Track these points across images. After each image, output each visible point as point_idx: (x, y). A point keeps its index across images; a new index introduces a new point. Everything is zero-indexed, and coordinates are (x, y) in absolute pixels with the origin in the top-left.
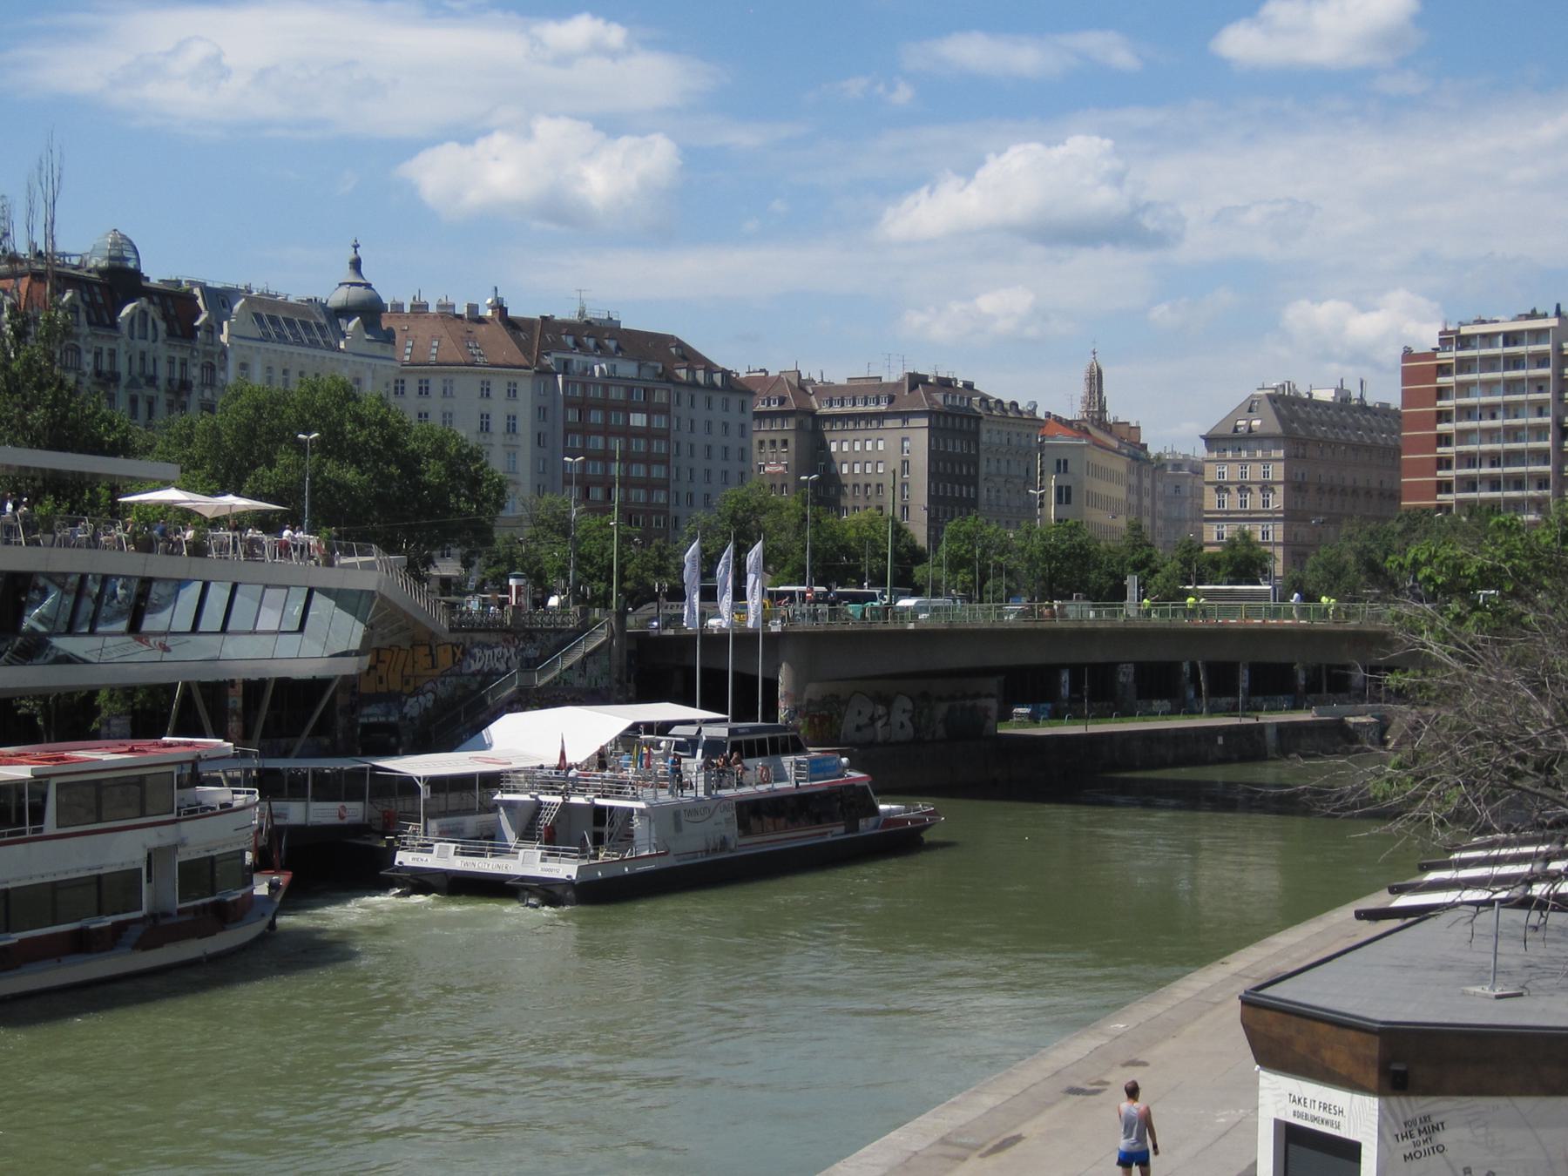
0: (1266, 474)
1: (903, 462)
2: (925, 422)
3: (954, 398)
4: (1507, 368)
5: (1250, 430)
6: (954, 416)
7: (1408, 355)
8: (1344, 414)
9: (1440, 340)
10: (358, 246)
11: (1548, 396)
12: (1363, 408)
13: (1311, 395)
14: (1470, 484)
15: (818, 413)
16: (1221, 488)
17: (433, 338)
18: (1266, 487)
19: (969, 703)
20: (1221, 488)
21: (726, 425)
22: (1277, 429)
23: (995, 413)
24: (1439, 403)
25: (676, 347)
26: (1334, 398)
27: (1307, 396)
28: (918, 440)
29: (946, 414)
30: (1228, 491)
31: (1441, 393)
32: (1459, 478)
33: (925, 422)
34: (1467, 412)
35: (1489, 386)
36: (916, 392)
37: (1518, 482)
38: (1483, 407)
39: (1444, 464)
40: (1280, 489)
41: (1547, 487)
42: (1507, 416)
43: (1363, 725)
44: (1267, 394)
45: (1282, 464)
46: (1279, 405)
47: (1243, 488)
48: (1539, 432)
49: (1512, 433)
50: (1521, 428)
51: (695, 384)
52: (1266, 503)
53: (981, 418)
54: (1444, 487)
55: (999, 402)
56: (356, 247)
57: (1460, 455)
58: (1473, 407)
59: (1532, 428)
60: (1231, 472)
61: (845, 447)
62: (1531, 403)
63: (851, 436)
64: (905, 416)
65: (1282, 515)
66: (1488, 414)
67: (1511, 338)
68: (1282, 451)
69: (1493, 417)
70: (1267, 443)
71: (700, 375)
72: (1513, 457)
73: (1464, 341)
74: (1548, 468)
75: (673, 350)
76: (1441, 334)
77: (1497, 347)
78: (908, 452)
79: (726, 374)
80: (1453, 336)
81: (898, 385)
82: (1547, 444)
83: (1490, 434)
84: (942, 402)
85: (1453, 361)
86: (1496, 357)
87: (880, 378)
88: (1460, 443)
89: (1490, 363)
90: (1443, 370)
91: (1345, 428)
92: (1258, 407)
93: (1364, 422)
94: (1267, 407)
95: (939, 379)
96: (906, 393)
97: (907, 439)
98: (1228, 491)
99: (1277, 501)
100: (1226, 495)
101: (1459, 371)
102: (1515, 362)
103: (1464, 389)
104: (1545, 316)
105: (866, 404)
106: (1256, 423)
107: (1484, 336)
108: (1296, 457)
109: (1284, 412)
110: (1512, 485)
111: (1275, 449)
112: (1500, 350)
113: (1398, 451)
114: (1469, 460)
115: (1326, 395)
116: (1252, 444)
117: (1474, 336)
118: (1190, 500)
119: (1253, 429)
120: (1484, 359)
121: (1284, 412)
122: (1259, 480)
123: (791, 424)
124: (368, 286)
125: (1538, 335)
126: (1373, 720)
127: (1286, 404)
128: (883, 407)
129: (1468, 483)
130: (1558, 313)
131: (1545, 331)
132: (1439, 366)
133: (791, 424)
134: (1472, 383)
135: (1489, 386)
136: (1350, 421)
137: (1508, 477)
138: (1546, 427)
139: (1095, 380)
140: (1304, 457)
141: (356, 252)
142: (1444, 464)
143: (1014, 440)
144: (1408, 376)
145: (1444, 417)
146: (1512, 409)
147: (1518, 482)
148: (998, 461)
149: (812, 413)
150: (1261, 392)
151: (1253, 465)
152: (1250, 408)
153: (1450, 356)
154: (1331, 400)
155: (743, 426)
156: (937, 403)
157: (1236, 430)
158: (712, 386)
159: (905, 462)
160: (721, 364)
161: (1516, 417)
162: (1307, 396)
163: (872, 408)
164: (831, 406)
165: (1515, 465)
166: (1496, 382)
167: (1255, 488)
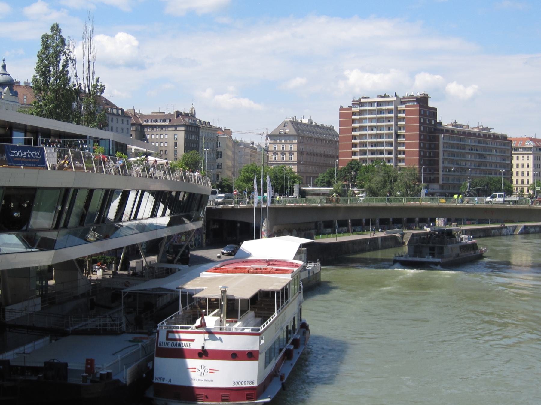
0: (291, 148)
1: (175, 142)
2: (183, 128)
3: (192, 120)
4: (378, 114)
5: (285, 133)
6: (192, 126)
7: (342, 108)
8: (312, 128)
9: (352, 103)
10: (5, 60)
11: (393, 123)
12: (316, 126)
13: (302, 121)
14: (364, 153)
15: (143, 124)
16: (275, 153)
17: (24, 95)
18: (291, 153)
19: (309, 232)
20: (275, 153)
21: (122, 129)
22: (294, 133)
23: (204, 126)
24: (353, 125)
25: (105, 100)
26: (308, 122)
27: (300, 122)
28: (181, 135)
29: (190, 126)
30: (277, 154)
31: (353, 122)
32: (360, 151)
33: (183, 128)
34: (362, 128)
35: (371, 120)
36: (179, 117)
37: (381, 153)
38: (369, 127)
40: (296, 154)
41: (391, 154)
42: (377, 130)
43: (398, 237)
44: (290, 121)
45: (297, 145)
47: (283, 153)
48: (389, 136)
49: (380, 136)
50: (383, 134)
51: (113, 114)
53: (200, 127)
54: (354, 153)
55: (204, 122)
56: (4, 60)
57: (361, 143)
59: (387, 134)
60: (279, 147)
61: (153, 137)
62: (386, 125)
63: (155, 133)
64: (175, 126)
65: (296, 162)
66: (370, 129)
67: (379, 104)
68: (297, 141)
69: (372, 130)
70: (286, 138)
71: (115, 111)
73: (362, 104)
74: (392, 148)
75: (104, 101)
76: (352, 101)
77: (374, 106)
78: (177, 139)
79: (122, 110)
81: (170, 115)
82: (392, 140)
83: (371, 136)
84: (188, 122)
85: (359, 111)
86: (374, 110)
87: (164, 113)
88: (361, 139)
89: (371, 112)
90: (354, 114)
91: (317, 133)
92: (287, 125)
94: (290, 125)
95: (185, 113)
96: (175, 118)
97: (177, 135)
98: (277, 154)
99: (295, 157)
100: (277, 155)
101: (361, 114)
102: (380, 112)
103: (362, 120)
104: (392, 97)
105: (161, 122)
106: (287, 131)
107: (369, 102)
108: (301, 142)
109: (296, 127)
110: (379, 153)
112: (375, 107)
113: (338, 142)
114: (364, 144)
115: (305, 121)
117: (366, 103)
118: (244, 156)
119: (286, 133)
120: (370, 110)
121: (296, 127)
122: (288, 150)
123: (134, 128)
124: (9, 75)
125: (389, 103)
126: (400, 235)
127: (295, 123)
128: (167, 123)
129: (363, 152)
130: (396, 95)
131: (392, 101)
132: (353, 112)
133: (134, 128)
134: (366, 119)
135: (371, 120)
137: (378, 150)
138: (392, 134)
139: (455, 121)
140: (303, 143)
141: (4, 62)
143: (210, 136)
144: (342, 116)
146: (379, 128)
147: (381, 153)
148: (208, 143)
149: (140, 125)
150: (287, 120)
151: (286, 145)
152: (285, 125)
153: (358, 109)
154: (307, 123)
155: (128, 129)
156: (187, 122)
157: (280, 133)
158: (118, 115)
159: (176, 143)
160: (119, 107)
161: (380, 130)
162: (300, 122)
163: (163, 123)
164: (156, 122)
165: (380, 147)
166: (374, 118)
167: (287, 153)
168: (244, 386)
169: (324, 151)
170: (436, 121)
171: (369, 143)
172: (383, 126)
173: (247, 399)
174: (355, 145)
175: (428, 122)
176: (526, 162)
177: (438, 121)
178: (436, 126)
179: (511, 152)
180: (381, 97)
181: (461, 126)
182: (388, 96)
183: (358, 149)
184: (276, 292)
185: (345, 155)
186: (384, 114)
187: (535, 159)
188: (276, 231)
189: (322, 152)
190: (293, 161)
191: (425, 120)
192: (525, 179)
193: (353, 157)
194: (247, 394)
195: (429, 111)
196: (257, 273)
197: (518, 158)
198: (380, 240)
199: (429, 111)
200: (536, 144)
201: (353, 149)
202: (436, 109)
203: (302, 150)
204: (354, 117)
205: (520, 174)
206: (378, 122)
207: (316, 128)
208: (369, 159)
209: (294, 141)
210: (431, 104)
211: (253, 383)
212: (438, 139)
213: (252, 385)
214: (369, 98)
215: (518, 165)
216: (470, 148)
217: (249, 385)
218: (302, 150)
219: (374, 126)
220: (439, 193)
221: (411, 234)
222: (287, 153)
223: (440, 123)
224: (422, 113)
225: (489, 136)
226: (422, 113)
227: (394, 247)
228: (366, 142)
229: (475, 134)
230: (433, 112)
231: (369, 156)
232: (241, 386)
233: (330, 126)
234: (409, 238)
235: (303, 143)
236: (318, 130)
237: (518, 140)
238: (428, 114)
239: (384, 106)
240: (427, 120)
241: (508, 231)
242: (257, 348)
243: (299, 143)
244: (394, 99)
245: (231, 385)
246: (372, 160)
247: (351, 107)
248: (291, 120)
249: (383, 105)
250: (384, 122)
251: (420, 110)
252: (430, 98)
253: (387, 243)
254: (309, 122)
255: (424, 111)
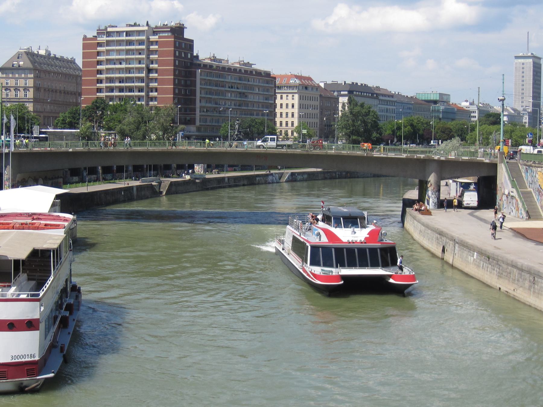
0: (26, 84)
4: (126, 45)
5: (19, 66)
7: (85, 38)
8: (50, 60)
9: (97, 33)
11: (144, 56)
12: (55, 58)
14: (111, 90)
18: (26, 89)
19: (56, 180)
22: (30, 65)
24: (98, 58)
26: (46, 53)
27: (37, 53)
31: (99, 54)
32: (107, 87)
34: (109, 61)
35: (119, 52)
37: (131, 90)
39: (99, 81)
40: (32, 90)
41: (142, 92)
42: (126, 64)
43: (155, 185)
44: (25, 52)
45: (32, 80)
46: (29, 56)
47: (16, 89)
48: (139, 70)
49: (129, 70)
50: (133, 68)
52: (26, 95)
54: (99, 90)
57: (107, 78)
58: (113, 60)
62: (136, 59)
65: (32, 100)
66: (118, 63)
67: (128, 33)
68: (33, 75)
69: (121, 64)
72: (131, 80)
73: (109, 34)
74: (143, 84)
76: (97, 30)
77: (123, 36)
80: (105, 31)
82: (143, 75)
86: (123, 41)
88: (107, 74)
89: (119, 43)
90: (100, 45)
91: (56, 67)
92: (21, 57)
93: (57, 64)
94: (25, 56)
99: (30, 94)
101: (107, 45)
102: (130, 43)
103: (108, 52)
104: (143, 26)
107: (117, 32)
108: (37, 77)
110: (128, 90)
111: (30, 74)
112: (124, 38)
113: (81, 77)
114: (111, 80)
115: (42, 52)
116: (20, 71)
117: (113, 32)
119: (20, 65)
120: (117, 41)
122: (23, 86)
125: (139, 33)
126: (157, 184)
127: (30, 54)
129: (110, 89)
130: (147, 25)
131: (143, 31)
132: (98, 43)
134: (113, 50)
135: (119, 52)
136: (53, 63)
137: (126, 87)
138: (143, 68)
140: (40, 77)
142: (99, 81)
144: (85, 46)
145: (99, 63)
146: (127, 61)
147: (131, 90)
150: (21, 51)
151: (20, 80)
152: (18, 56)
154: (44, 54)
157: (13, 66)
161: (130, 64)
162: (37, 53)
165: (129, 83)
166: (123, 50)
167: (21, 89)
168: (23, 360)
169: (65, 87)
170: (192, 54)
171: (116, 78)
172: (133, 59)
173: (28, 375)
174: (100, 81)
175: (183, 55)
176: (290, 102)
177: (195, 54)
178: (192, 60)
179: (275, 90)
180: (131, 26)
181: (220, 61)
182: (139, 25)
183: (103, 85)
184: (52, 251)
185: (90, 92)
186: (134, 45)
187: (300, 98)
188: (20, 180)
189: (62, 89)
190: (28, 99)
191: (180, 53)
192: (290, 120)
193: (98, 94)
194: (27, 370)
195: (185, 44)
196: (23, 229)
197: (281, 98)
198: (135, 189)
199: (185, 44)
200: (302, 82)
201: (98, 85)
202: (192, 41)
203: (38, 86)
204: (99, 49)
205: (284, 115)
206: (127, 54)
207: (54, 61)
208: (116, 96)
209: (29, 76)
210: (187, 35)
211: (34, 356)
212: (194, 75)
213: (33, 359)
214: (116, 27)
215: (281, 105)
216: (230, 85)
217: (29, 359)
218: (38, 86)
219: (123, 60)
220: (196, 136)
221: (170, 182)
222: (21, 89)
223: (197, 57)
224: (177, 45)
225: (251, 72)
226: (177, 45)
227: (151, 197)
228: (113, 78)
229: (234, 70)
230: (190, 44)
231: (116, 94)
232: (20, 360)
233: (71, 59)
234: (167, 187)
235: (40, 77)
236: (57, 63)
237: (282, 77)
238: (183, 46)
239: (134, 36)
240: (183, 53)
241: (274, 178)
242: (37, 316)
243: (36, 78)
244: (146, 28)
245: (8, 360)
246: (120, 98)
247: (96, 37)
248: (26, 50)
249: (133, 36)
250: (134, 54)
251: (175, 42)
252: (187, 28)
253: (143, 193)
254: (47, 53)
255: (179, 43)
